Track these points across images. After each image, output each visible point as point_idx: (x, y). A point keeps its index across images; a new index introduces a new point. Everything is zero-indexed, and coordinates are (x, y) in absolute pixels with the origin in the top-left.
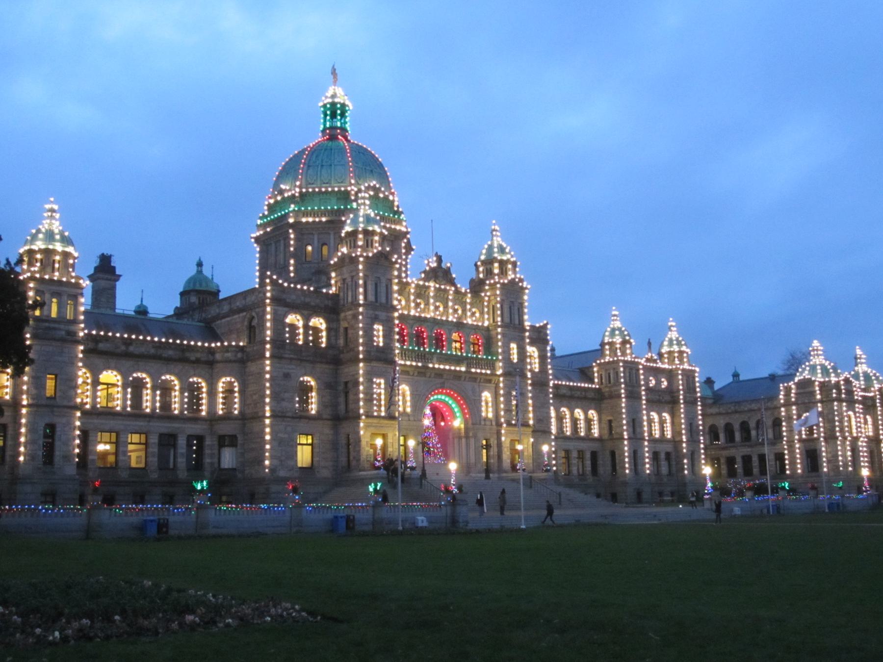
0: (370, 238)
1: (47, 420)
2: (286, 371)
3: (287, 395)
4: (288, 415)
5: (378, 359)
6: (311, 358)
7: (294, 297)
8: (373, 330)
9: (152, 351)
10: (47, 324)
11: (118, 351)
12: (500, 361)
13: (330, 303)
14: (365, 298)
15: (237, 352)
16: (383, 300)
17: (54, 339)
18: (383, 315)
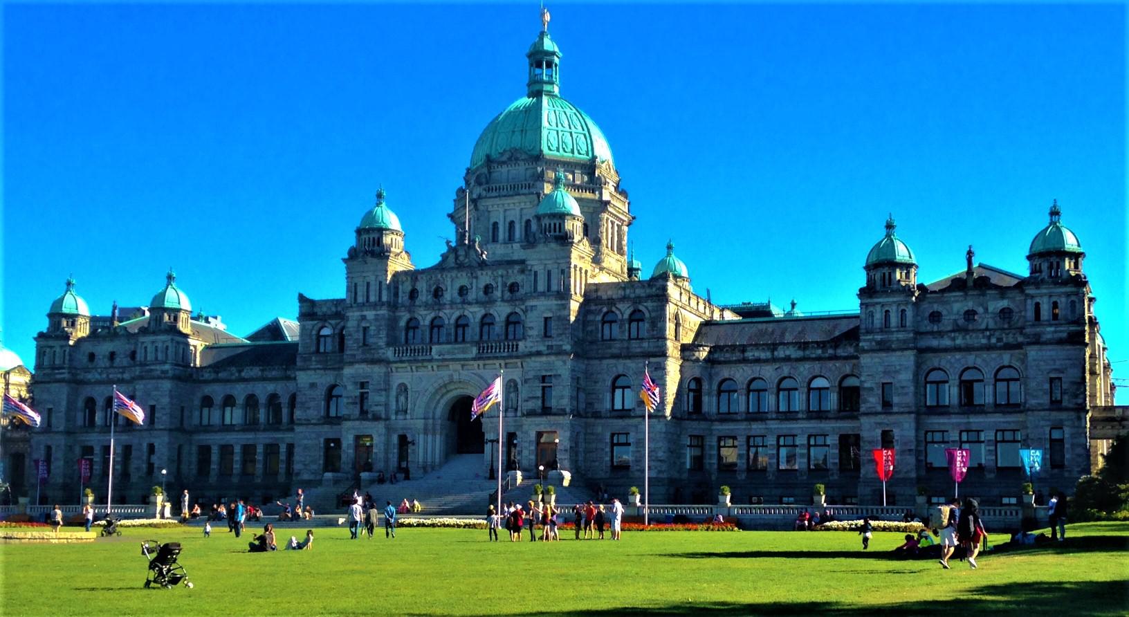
3: (312, 404)
7: (324, 309)
17: (153, 378)
18: (370, 314)
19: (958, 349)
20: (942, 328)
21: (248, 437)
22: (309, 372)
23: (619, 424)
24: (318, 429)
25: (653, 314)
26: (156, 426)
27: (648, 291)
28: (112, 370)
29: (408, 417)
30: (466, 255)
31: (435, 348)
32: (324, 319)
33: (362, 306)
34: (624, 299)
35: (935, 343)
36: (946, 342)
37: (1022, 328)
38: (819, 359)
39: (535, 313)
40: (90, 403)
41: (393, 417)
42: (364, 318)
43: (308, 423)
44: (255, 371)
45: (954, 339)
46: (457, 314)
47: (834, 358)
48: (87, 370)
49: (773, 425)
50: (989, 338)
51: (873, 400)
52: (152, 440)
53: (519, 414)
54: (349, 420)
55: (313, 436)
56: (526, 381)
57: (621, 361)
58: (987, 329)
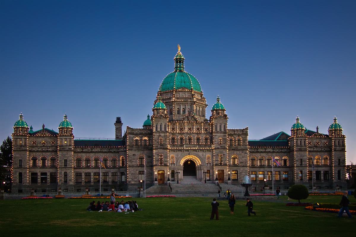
0: (158, 111)
1: (65, 171)
2: (133, 153)
3: (134, 160)
4: (134, 166)
5: (161, 148)
6: (143, 149)
8: (158, 139)
9: (100, 150)
10: (63, 147)
11: (90, 151)
12: (214, 144)
13: (149, 132)
14: (156, 130)
15: (124, 149)
16: (163, 130)
18: (162, 134)
19: (315, 151)
20: (312, 146)
21: (96, 170)
22: (133, 151)
23: (235, 168)
24: (137, 168)
25: (244, 139)
26: (68, 166)
27: (242, 132)
28: (44, 147)
29: (175, 165)
30: (191, 119)
31: (184, 146)
32: (137, 135)
33: (159, 132)
34: (235, 134)
35: (310, 149)
36: (312, 149)
37: (329, 147)
38: (277, 152)
39: (216, 137)
40: (34, 160)
41: (170, 165)
42: (160, 135)
43: (133, 166)
44: (99, 150)
45: (314, 149)
46: (188, 136)
47: (281, 152)
48: (33, 147)
49: (266, 169)
50: (322, 149)
51: (298, 163)
52: (67, 171)
53: (211, 165)
54: (156, 166)
55: (135, 170)
56: (215, 156)
57: (235, 151)
58: (322, 147)
